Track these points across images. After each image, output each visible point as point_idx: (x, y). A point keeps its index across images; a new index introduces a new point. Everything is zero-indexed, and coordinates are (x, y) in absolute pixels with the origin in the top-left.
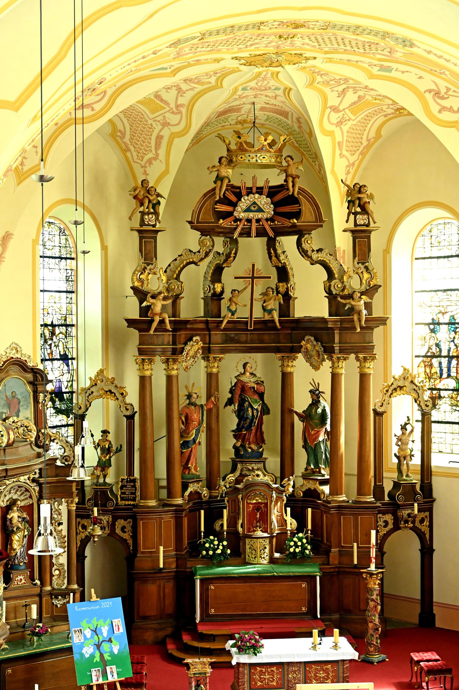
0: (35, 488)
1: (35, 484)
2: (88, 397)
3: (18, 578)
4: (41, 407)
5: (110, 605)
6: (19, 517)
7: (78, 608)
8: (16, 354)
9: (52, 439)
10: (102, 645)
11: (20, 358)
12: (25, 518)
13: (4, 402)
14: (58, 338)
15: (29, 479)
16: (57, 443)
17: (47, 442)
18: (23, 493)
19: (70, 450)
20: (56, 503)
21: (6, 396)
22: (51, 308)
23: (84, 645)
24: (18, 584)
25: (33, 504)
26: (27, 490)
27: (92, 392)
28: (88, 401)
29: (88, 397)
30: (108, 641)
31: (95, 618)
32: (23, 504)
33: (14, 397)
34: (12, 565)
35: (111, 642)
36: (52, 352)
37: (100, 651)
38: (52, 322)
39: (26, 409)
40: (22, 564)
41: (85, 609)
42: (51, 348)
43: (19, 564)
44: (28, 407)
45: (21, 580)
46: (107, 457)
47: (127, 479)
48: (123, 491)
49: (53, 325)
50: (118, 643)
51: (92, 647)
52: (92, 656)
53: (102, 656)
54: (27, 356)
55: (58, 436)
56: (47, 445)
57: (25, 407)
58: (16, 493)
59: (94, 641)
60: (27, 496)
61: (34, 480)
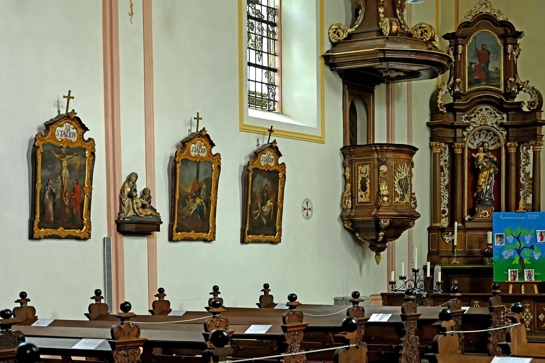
0: (503, 132)
1: (503, 129)
3: (483, 212)
4: (510, 58)
5: (536, 217)
6: (485, 157)
8: (485, 10)
9: (520, 87)
10: (523, 250)
11: (490, 13)
12: (491, 158)
13: (474, 54)
15: (496, 123)
16: (525, 91)
17: (513, 89)
19: (535, 96)
20: (525, 147)
21: (476, 48)
24: (482, 218)
25: (500, 148)
26: (495, 134)
30: (530, 248)
32: (492, 148)
33: (483, 49)
34: (479, 201)
35: (533, 249)
39: (496, 60)
40: (487, 200)
43: (485, 199)
44: (498, 58)
45: (486, 214)
51: (513, 251)
52: (512, 259)
53: (521, 260)
54: (497, 11)
55: (526, 84)
56: (513, 91)
58: (486, 137)
59: (515, 246)
60: (496, 141)
61: (501, 125)
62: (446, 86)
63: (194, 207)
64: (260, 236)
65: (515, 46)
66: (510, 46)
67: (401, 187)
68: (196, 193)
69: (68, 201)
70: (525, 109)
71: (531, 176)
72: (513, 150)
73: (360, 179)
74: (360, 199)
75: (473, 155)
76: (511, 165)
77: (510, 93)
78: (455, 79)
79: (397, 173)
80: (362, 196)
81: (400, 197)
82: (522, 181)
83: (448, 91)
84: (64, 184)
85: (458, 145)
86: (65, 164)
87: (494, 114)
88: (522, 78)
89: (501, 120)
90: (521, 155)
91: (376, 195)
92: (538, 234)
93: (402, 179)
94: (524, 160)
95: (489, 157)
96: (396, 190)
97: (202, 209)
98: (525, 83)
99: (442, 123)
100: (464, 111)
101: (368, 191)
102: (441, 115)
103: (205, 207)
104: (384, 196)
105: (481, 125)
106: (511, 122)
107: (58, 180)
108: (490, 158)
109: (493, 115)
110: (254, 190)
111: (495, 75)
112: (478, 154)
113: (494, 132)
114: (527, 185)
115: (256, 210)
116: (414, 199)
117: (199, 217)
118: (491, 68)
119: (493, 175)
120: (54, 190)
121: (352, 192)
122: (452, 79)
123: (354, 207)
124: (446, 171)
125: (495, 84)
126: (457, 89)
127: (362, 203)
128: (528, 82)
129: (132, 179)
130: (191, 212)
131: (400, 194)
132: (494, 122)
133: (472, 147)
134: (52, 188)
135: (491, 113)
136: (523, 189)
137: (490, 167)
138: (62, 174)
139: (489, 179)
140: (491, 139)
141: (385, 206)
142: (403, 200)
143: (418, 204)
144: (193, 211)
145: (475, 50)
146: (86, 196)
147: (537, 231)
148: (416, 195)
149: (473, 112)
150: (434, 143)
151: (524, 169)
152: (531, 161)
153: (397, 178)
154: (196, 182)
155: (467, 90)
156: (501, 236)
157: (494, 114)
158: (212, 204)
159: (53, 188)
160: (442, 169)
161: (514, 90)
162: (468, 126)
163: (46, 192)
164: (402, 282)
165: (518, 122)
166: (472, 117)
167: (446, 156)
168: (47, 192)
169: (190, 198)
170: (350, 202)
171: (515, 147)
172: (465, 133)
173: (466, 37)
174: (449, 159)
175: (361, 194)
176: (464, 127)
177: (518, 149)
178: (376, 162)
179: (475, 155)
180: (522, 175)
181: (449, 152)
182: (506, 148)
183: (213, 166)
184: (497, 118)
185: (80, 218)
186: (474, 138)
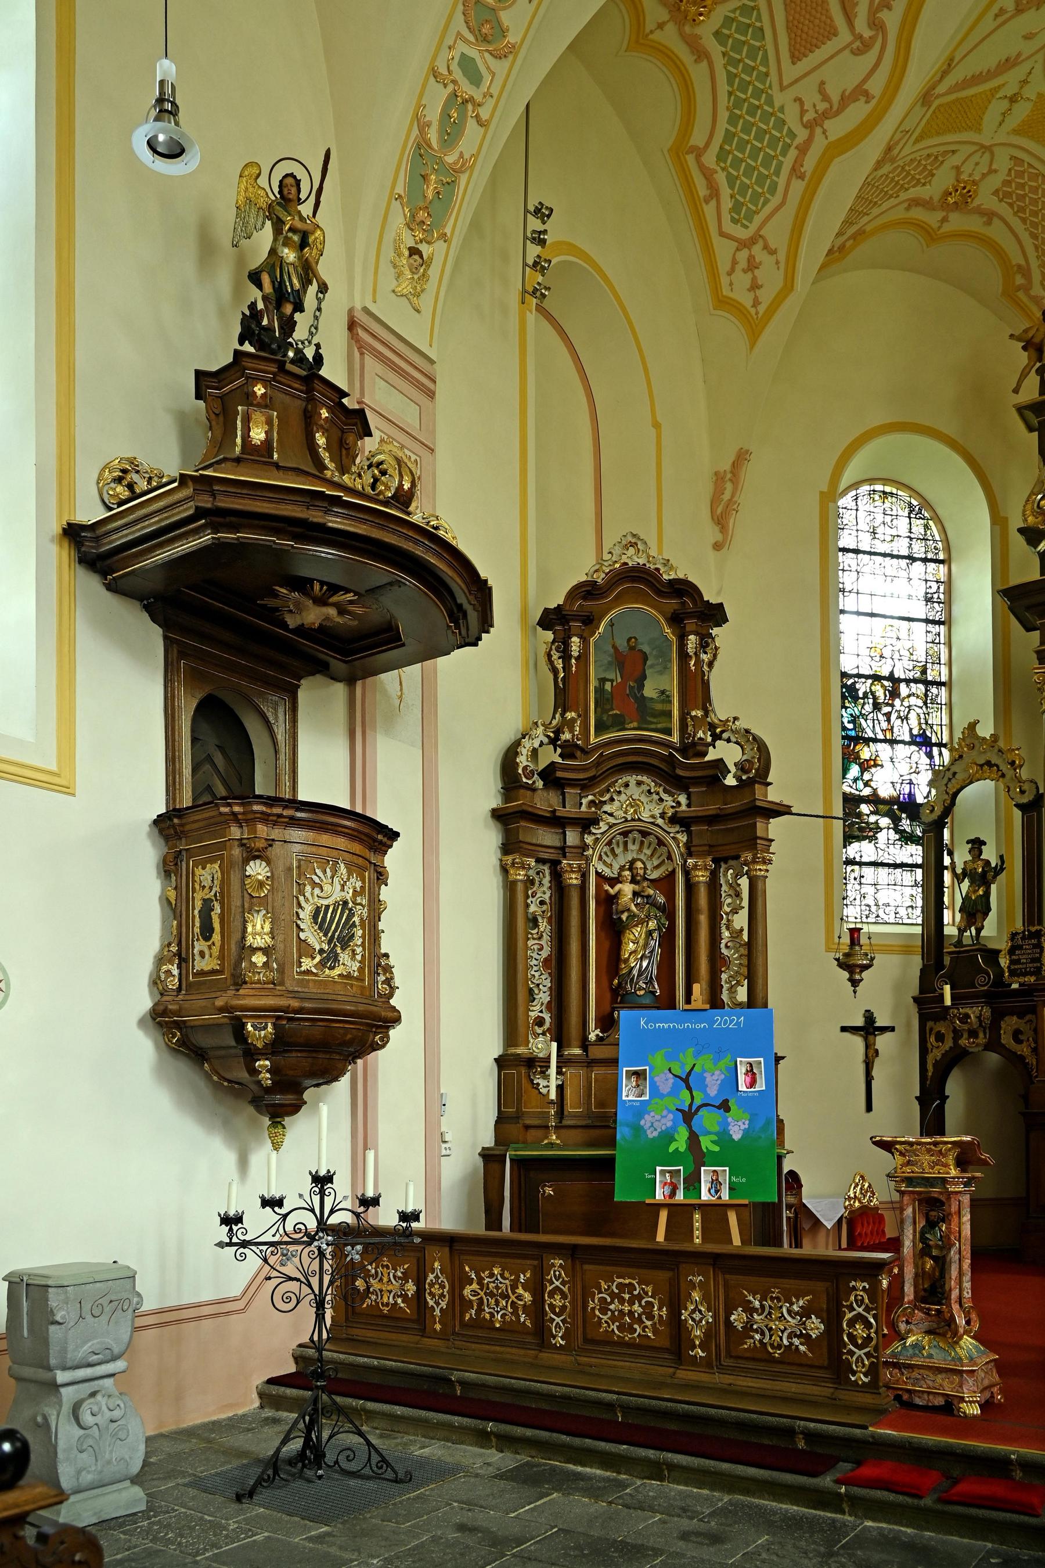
0: (679, 836)
1: (677, 828)
2: (946, 785)
6: (635, 894)
7: (646, 1023)
9: (718, 730)
10: (700, 1113)
14: (906, 704)
15: (662, 815)
16: (729, 741)
17: (700, 734)
18: (642, 843)
20: (731, 871)
21: (614, 647)
22: (891, 648)
23: (649, 1108)
25: (674, 872)
26: (661, 843)
27: (955, 774)
28: (947, 793)
29: (946, 785)
30: (719, 1107)
31: (691, 1050)
32: (655, 875)
33: (632, 648)
35: (728, 1109)
36: (892, 727)
37: (690, 1127)
38: (892, 673)
39: (661, 673)
41: (666, 1026)
42: (889, 720)
44: (665, 668)
46: (981, 892)
47: (1024, 932)
48: (1014, 957)
49: (891, 678)
50: (747, 1116)
51: (671, 1116)
53: (694, 1140)
56: (701, 739)
57: (658, 668)
58: (640, 850)
59: (678, 1102)
60: (664, 857)
61: (674, 820)
62: (541, 729)
65: (705, 641)
66: (692, 637)
67: (320, 928)
70: (730, 781)
71: (745, 937)
72: (701, 877)
73: (198, 904)
74: (201, 964)
75: (607, 887)
76: (698, 911)
77: (694, 744)
78: (562, 715)
79: (308, 888)
80: (202, 954)
81: (318, 958)
82: (724, 951)
83: (546, 740)
85: (570, 865)
87: (658, 794)
88: (722, 709)
89: (672, 807)
90: (723, 889)
91: (233, 947)
92: (742, 1070)
93: (327, 907)
94: (729, 900)
95: (646, 894)
96: (302, 936)
98: (727, 720)
99: (525, 808)
100: (585, 786)
101: (216, 937)
102: (529, 793)
104: (254, 950)
105: (626, 821)
106: (696, 810)
108: (648, 897)
109: (655, 797)
111: (659, 707)
112: (618, 886)
113: (657, 838)
114: (736, 959)
116: (388, 969)
118: (650, 691)
119: (655, 935)
121: (179, 944)
122: (558, 716)
123: (184, 986)
124: (543, 925)
125: (659, 726)
126: (566, 736)
127: (202, 973)
128: (735, 719)
131: (318, 948)
132: (657, 812)
133: (607, 872)
135: (649, 791)
136: (728, 968)
137: (648, 917)
139: (646, 945)
140: (652, 855)
141: (259, 982)
142: (331, 968)
143: (397, 982)
145: (612, 650)
147: (739, 1059)
148: (392, 961)
149: (608, 791)
150: (509, 859)
151: (728, 920)
152: (745, 903)
153: (307, 900)
155: (592, 740)
156: (639, 1075)
157: (658, 794)
160: (534, 922)
161: (702, 736)
162: (595, 821)
164: (269, 1216)
165: (712, 809)
166: (605, 802)
167: (544, 891)
170: (176, 972)
171: (706, 869)
172: (589, 840)
173: (590, 621)
174: (550, 898)
175: (201, 948)
176: (586, 824)
177: (714, 875)
178: (237, 852)
179: (612, 888)
180: (726, 934)
181: (550, 882)
182: (687, 873)
184: (665, 803)
186: (612, 850)
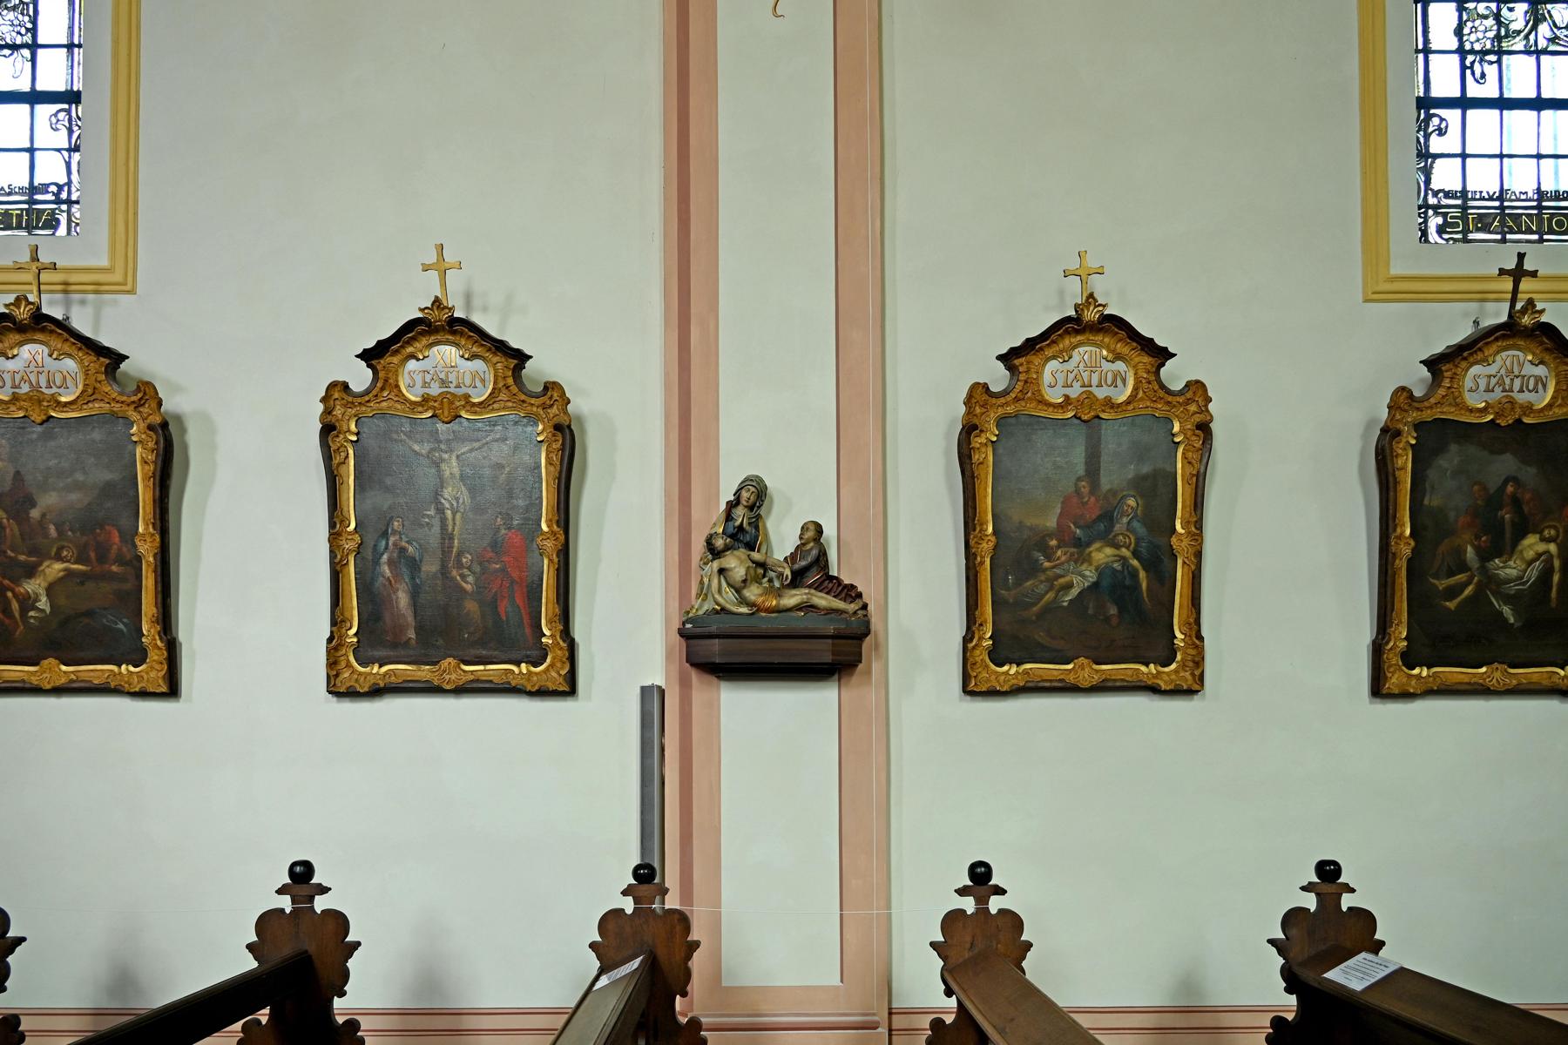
63: (1083, 576)
64: (1484, 669)
68: (1087, 527)
69: (470, 579)
84: (450, 528)
86: (452, 467)
97: (1128, 582)
103: (1142, 574)
107: (427, 520)
110: (1431, 501)
115: (1451, 574)
117: (1113, 611)
120: (410, 549)
129: (754, 496)
130: (1066, 594)
134: (404, 544)
138: (443, 501)
144: (1074, 592)
146: (546, 561)
154: (1085, 491)
158: (1180, 562)
159: (408, 542)
163: (383, 554)
168: (385, 557)
169: (1059, 547)
183: (1176, 428)
185: (528, 631)
